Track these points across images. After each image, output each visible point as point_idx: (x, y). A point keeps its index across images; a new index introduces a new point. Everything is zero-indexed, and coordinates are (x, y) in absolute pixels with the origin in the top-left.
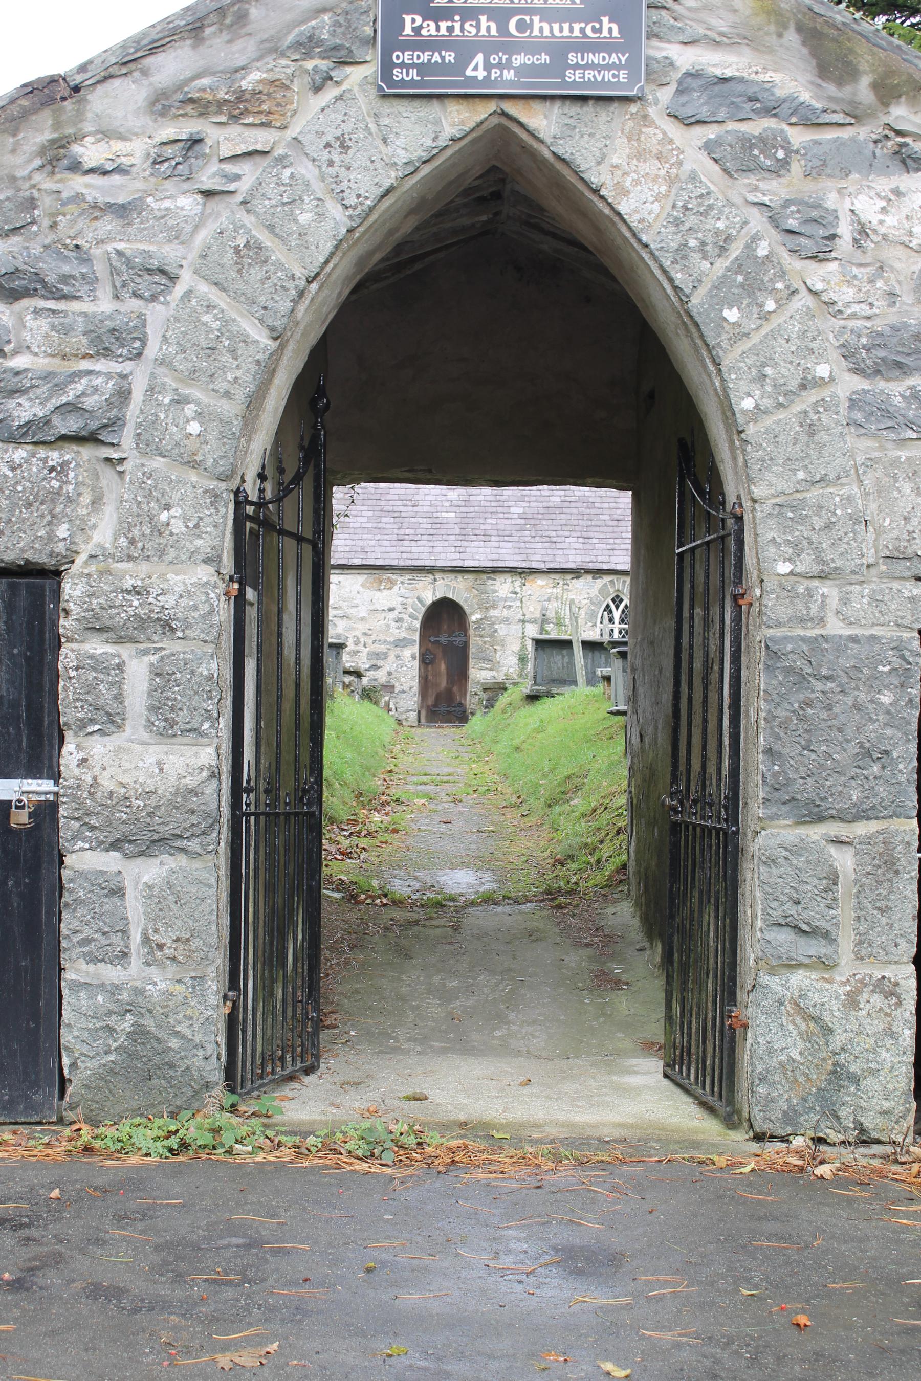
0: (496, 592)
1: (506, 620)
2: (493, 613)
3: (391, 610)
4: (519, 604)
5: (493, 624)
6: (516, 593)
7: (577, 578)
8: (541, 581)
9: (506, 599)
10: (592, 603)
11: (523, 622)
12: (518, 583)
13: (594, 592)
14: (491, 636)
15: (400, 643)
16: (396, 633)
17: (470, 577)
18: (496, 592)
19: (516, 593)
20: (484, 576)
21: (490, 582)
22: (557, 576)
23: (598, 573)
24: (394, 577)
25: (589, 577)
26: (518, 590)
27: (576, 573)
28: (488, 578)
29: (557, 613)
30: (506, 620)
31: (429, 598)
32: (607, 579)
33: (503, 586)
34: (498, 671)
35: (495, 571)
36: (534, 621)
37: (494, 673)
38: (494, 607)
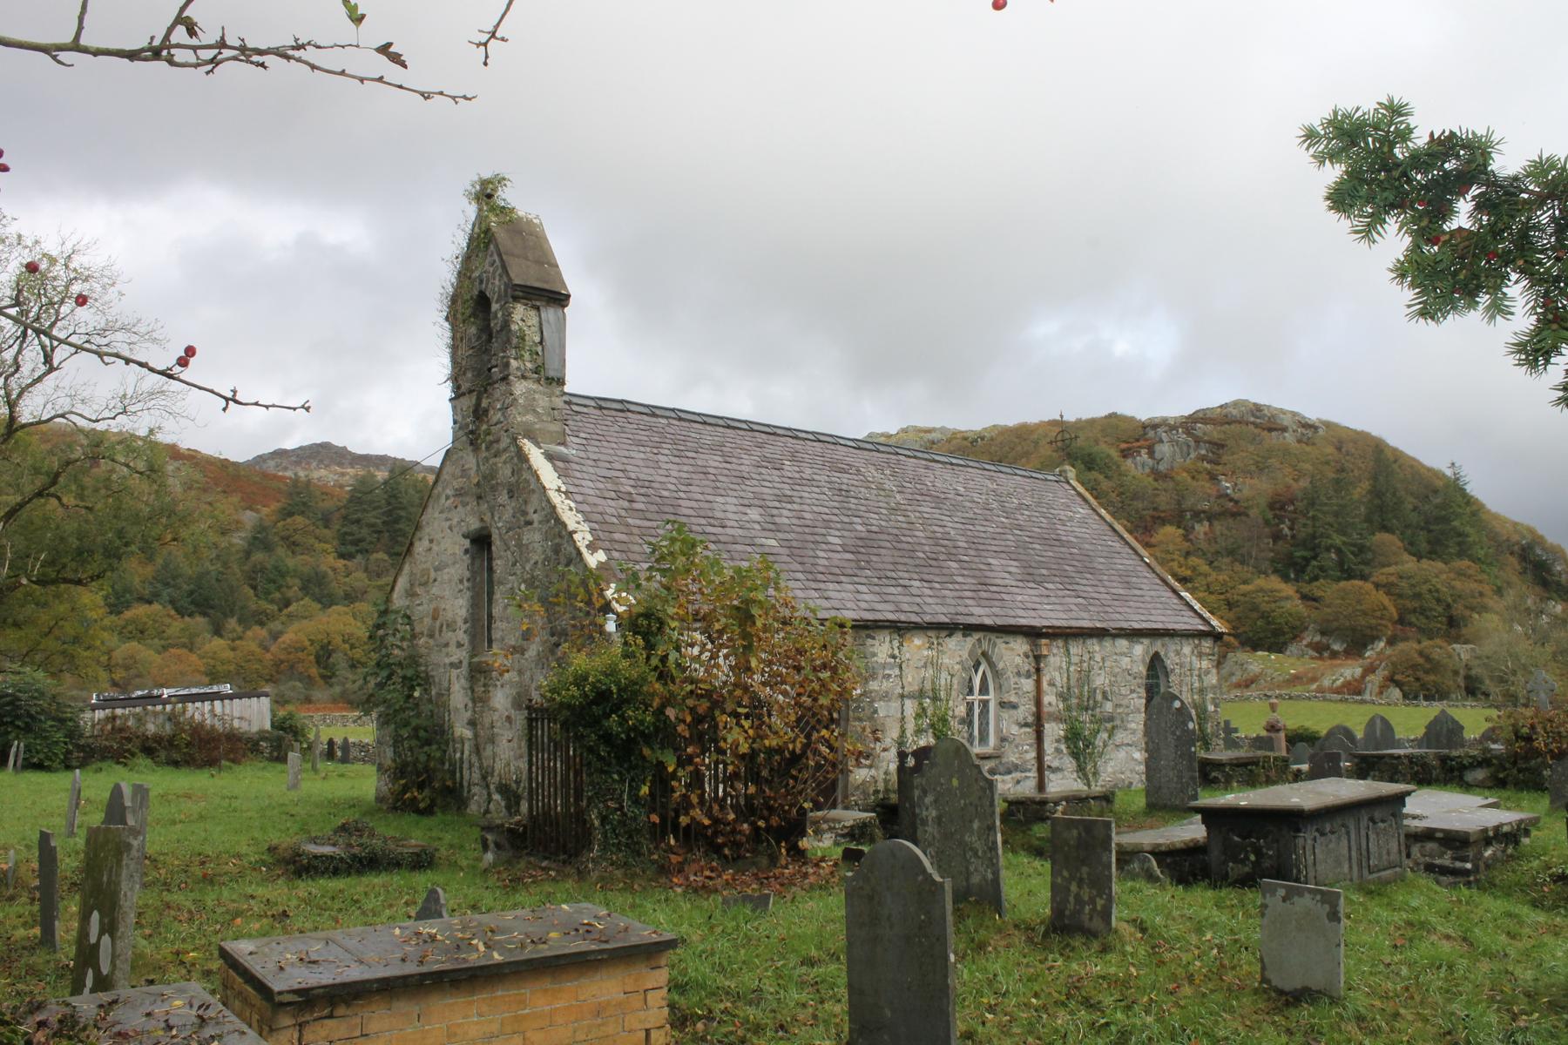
0: (874, 655)
1: (886, 696)
2: (873, 685)
4: (897, 671)
5: (872, 701)
6: (894, 657)
7: (950, 635)
8: (917, 642)
9: (884, 666)
11: (902, 696)
12: (896, 644)
14: (871, 719)
18: (874, 655)
19: (894, 657)
21: (869, 641)
23: (969, 629)
25: (958, 637)
26: (896, 652)
27: (950, 628)
28: (869, 636)
29: (933, 683)
30: (886, 696)
32: (976, 636)
33: (882, 648)
34: (877, 769)
36: (911, 696)
37: (873, 772)
38: (873, 676)
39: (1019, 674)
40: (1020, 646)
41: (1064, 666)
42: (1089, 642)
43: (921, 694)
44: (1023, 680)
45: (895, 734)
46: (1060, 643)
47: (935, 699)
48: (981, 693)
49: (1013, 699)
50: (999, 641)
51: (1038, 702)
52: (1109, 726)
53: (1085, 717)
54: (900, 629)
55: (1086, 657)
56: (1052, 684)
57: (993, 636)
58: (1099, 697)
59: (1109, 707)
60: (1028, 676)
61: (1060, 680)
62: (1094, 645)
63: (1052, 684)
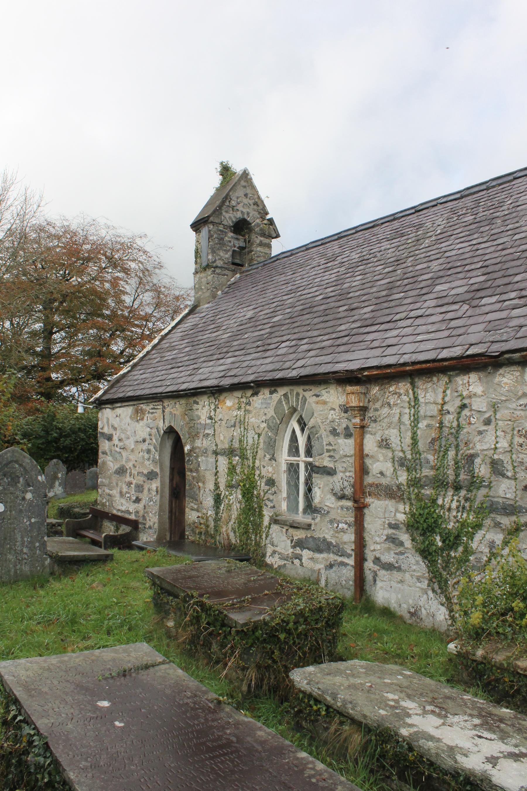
1: (205, 452)
2: (198, 443)
3: (144, 441)
5: (197, 457)
9: (205, 426)
10: (269, 427)
13: (271, 412)
14: (197, 471)
15: (151, 476)
16: (149, 466)
17: (183, 401)
20: (191, 400)
21: (195, 406)
22: (238, 394)
23: (274, 384)
24: (144, 407)
25: (266, 392)
26: (212, 413)
27: (256, 386)
31: (162, 426)
32: (282, 391)
35: (195, 393)
39: (334, 432)
40: (334, 397)
41: (406, 419)
42: (461, 380)
43: (230, 452)
44: (341, 441)
45: (211, 486)
46: (403, 386)
47: (243, 457)
48: (309, 452)
49: (327, 463)
50: (308, 394)
51: (362, 470)
52: (506, 521)
53: (449, 500)
54: (217, 392)
55: (452, 407)
56: (384, 444)
57: (299, 389)
58: (482, 470)
59: (505, 490)
60: (348, 435)
61: (399, 440)
62: (472, 384)
63: (384, 444)
